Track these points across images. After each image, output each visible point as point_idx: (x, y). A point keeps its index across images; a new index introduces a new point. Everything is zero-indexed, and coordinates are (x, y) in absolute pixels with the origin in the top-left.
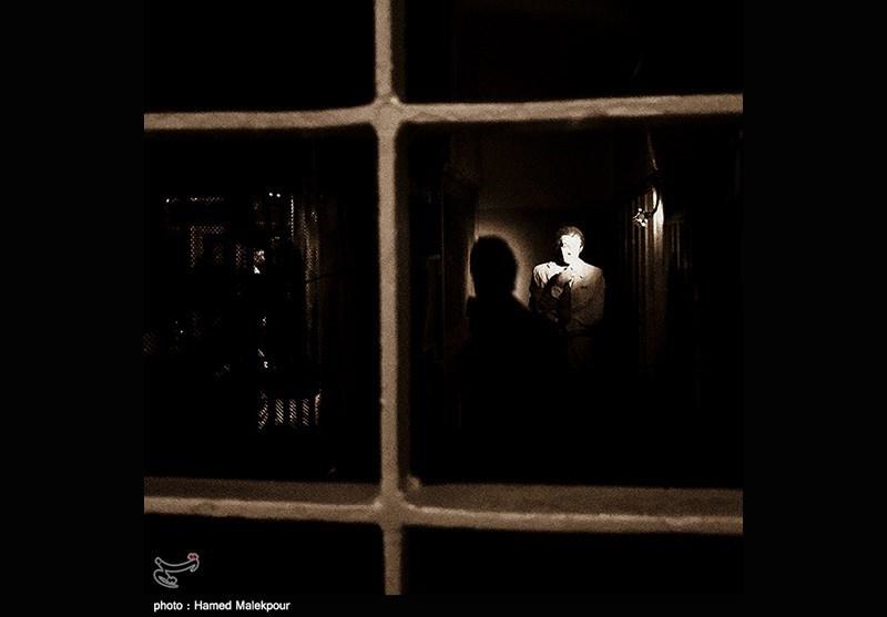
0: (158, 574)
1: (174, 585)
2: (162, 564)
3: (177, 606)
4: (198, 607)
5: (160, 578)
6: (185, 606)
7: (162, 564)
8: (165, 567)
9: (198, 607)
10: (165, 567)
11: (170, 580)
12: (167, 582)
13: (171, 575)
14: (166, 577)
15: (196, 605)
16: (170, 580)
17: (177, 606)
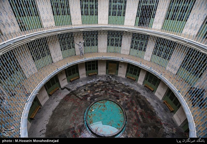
0: (3, 132)
1: (8, 135)
2: (4, 130)
3: (11, 141)
4: (20, 141)
5: (4, 133)
7: (4, 130)
8: (5, 130)
9: (20, 141)
10: (5, 130)
11: (6, 134)
12: (6, 135)
13: (7, 133)
14: (5, 133)
15: (20, 141)
16: (6, 134)
17: (11, 141)
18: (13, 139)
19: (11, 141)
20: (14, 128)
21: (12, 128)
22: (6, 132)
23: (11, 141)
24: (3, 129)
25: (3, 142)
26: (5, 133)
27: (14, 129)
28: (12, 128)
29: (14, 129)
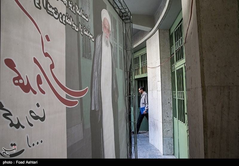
0: (3, 153)
2: (5, 150)
5: (4, 154)
6: (13, 163)
7: (5, 150)
10: (5, 150)
16: (7, 155)
18: (14, 160)
19: (11, 162)
20: (15, 147)
21: (14, 147)
22: (5, 152)
23: (11, 162)
24: (3, 148)
25: (3, 163)
26: (6, 154)
27: (15, 149)
28: (13, 147)
29: (15, 149)
